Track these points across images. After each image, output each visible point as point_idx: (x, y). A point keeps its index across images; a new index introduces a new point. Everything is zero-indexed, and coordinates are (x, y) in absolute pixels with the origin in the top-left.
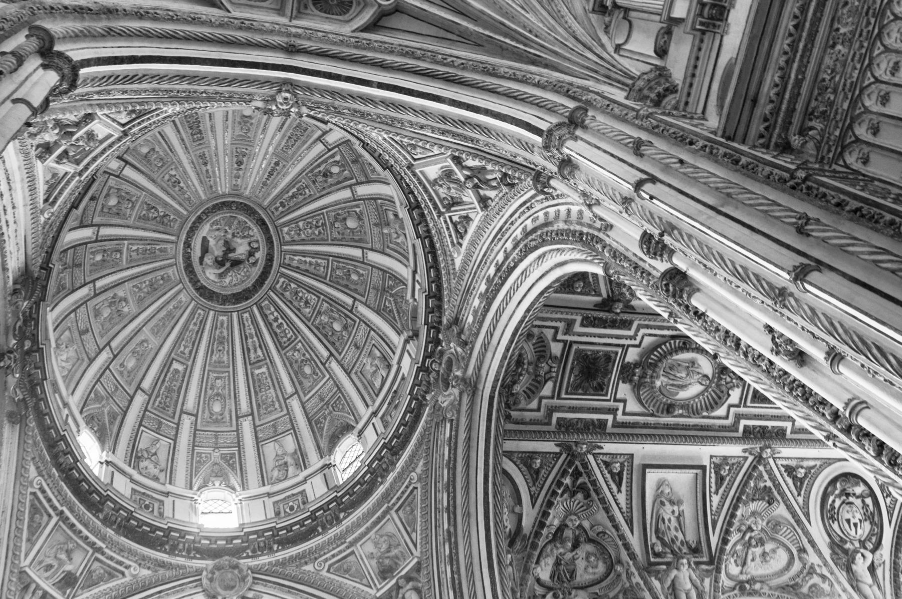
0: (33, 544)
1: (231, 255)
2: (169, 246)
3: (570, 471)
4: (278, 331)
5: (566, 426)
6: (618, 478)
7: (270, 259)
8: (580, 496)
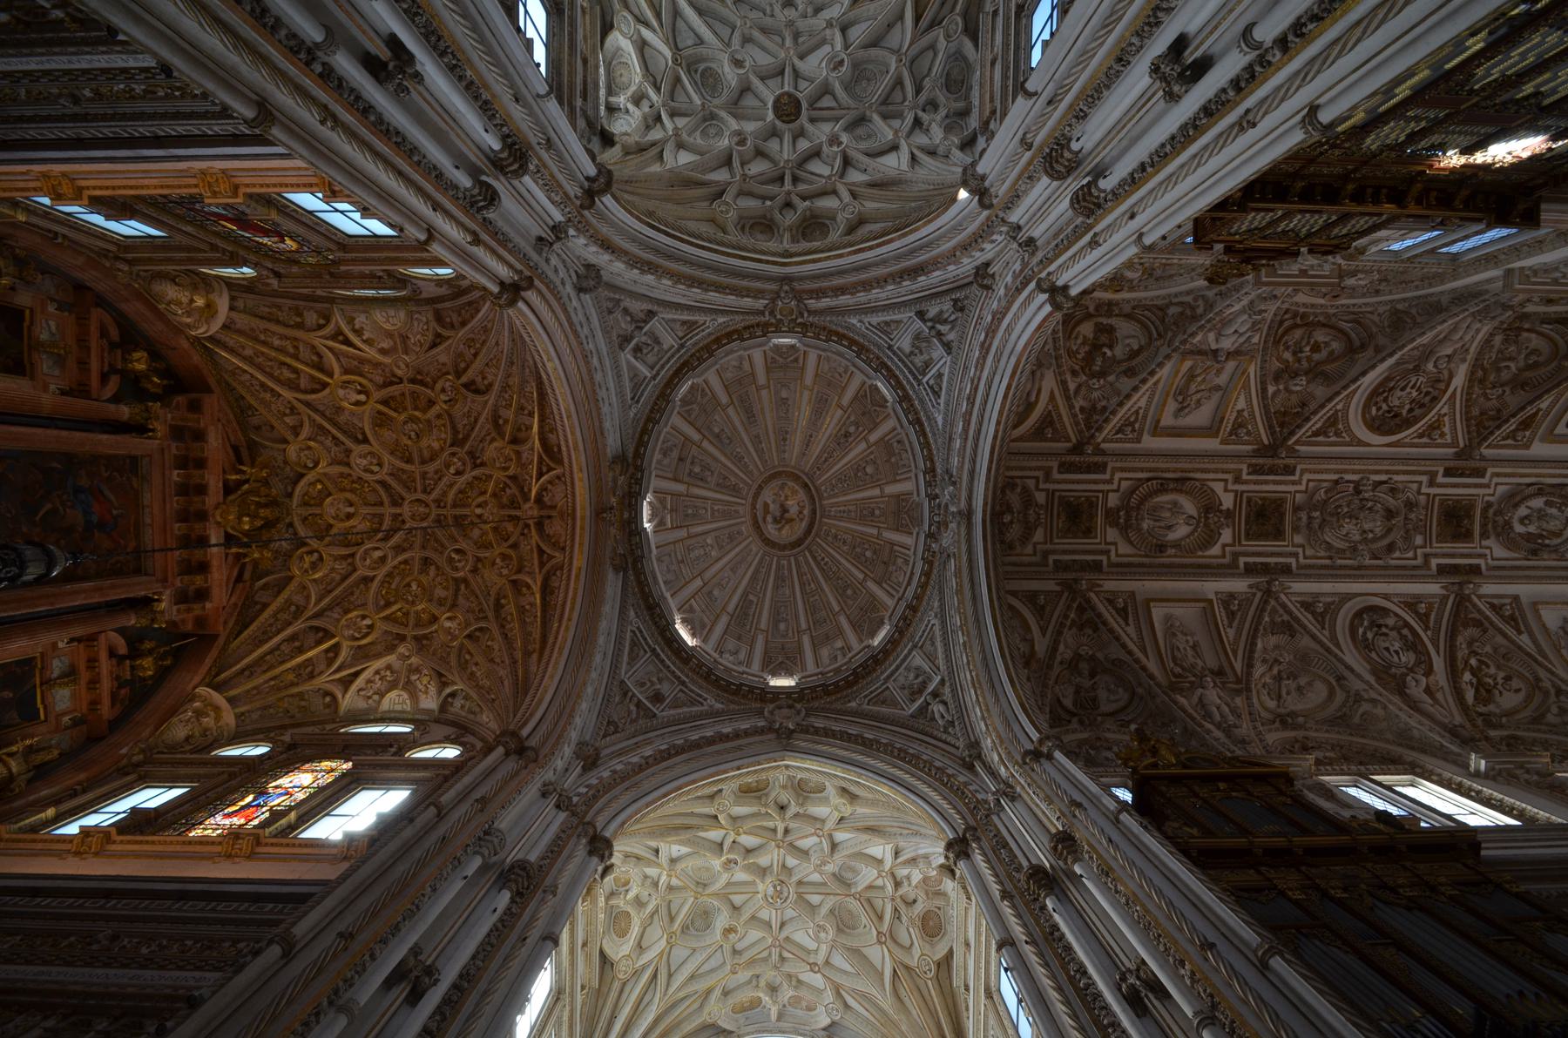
1: (786, 515)
3: (1075, 605)
5: (1060, 566)
6: (1123, 613)
8: (1089, 631)
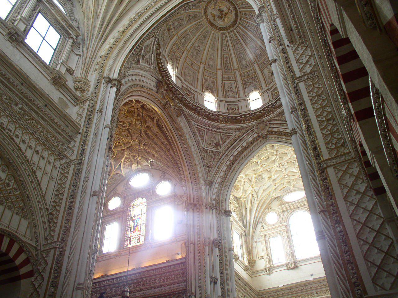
0: (203, 140)
1: (223, 12)
2: (202, 22)
4: (251, 30)
7: (235, 8)
